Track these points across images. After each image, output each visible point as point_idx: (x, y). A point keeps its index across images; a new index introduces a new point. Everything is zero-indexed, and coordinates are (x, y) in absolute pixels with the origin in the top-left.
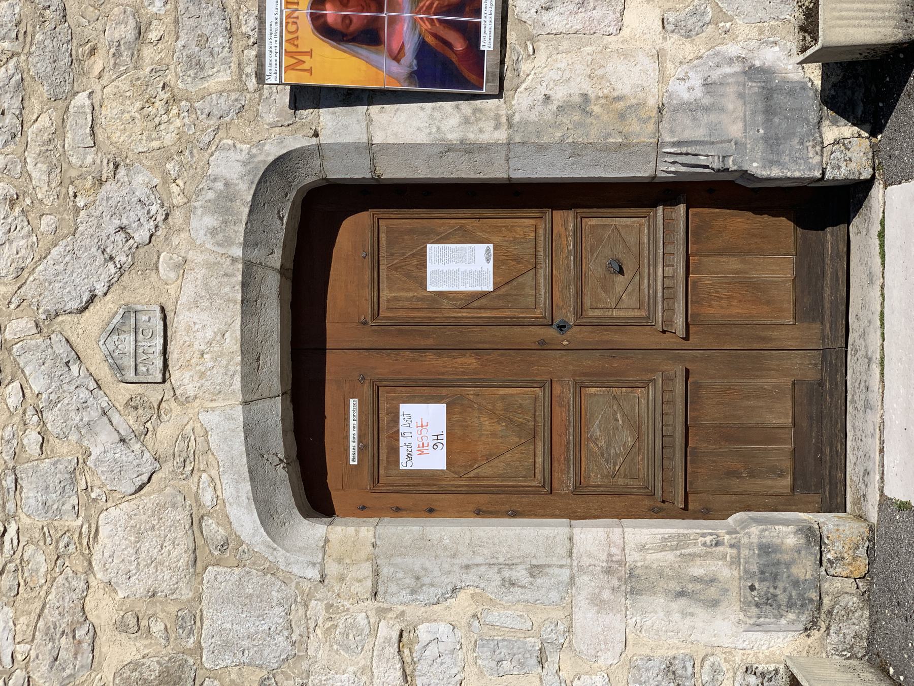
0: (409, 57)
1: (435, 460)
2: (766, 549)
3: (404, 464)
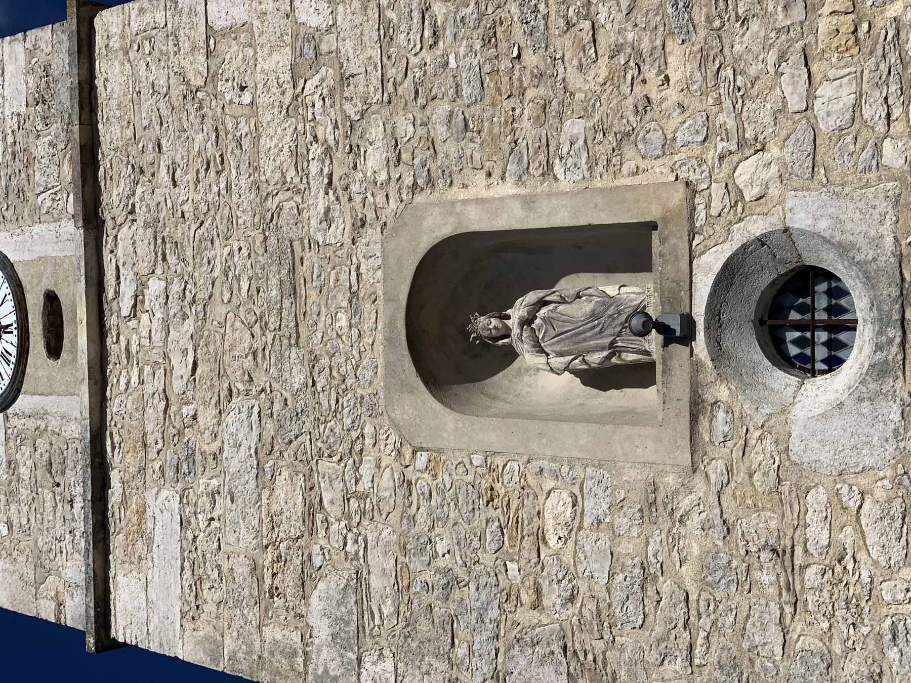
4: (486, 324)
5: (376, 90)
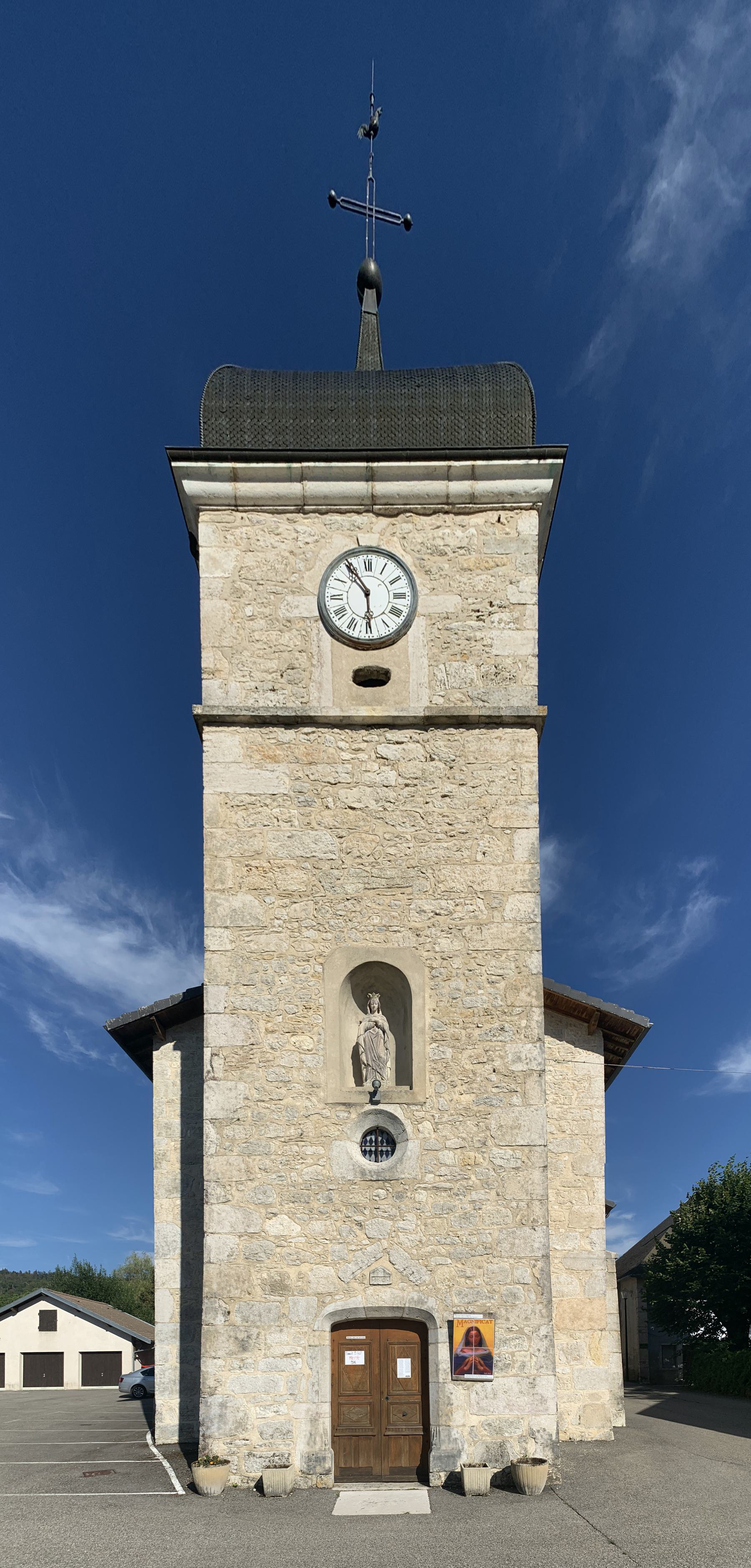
0: (462, 1354)
1: (348, 1362)
2: (324, 1458)
3: (347, 1352)
4: (375, 1001)
5: (474, 946)
